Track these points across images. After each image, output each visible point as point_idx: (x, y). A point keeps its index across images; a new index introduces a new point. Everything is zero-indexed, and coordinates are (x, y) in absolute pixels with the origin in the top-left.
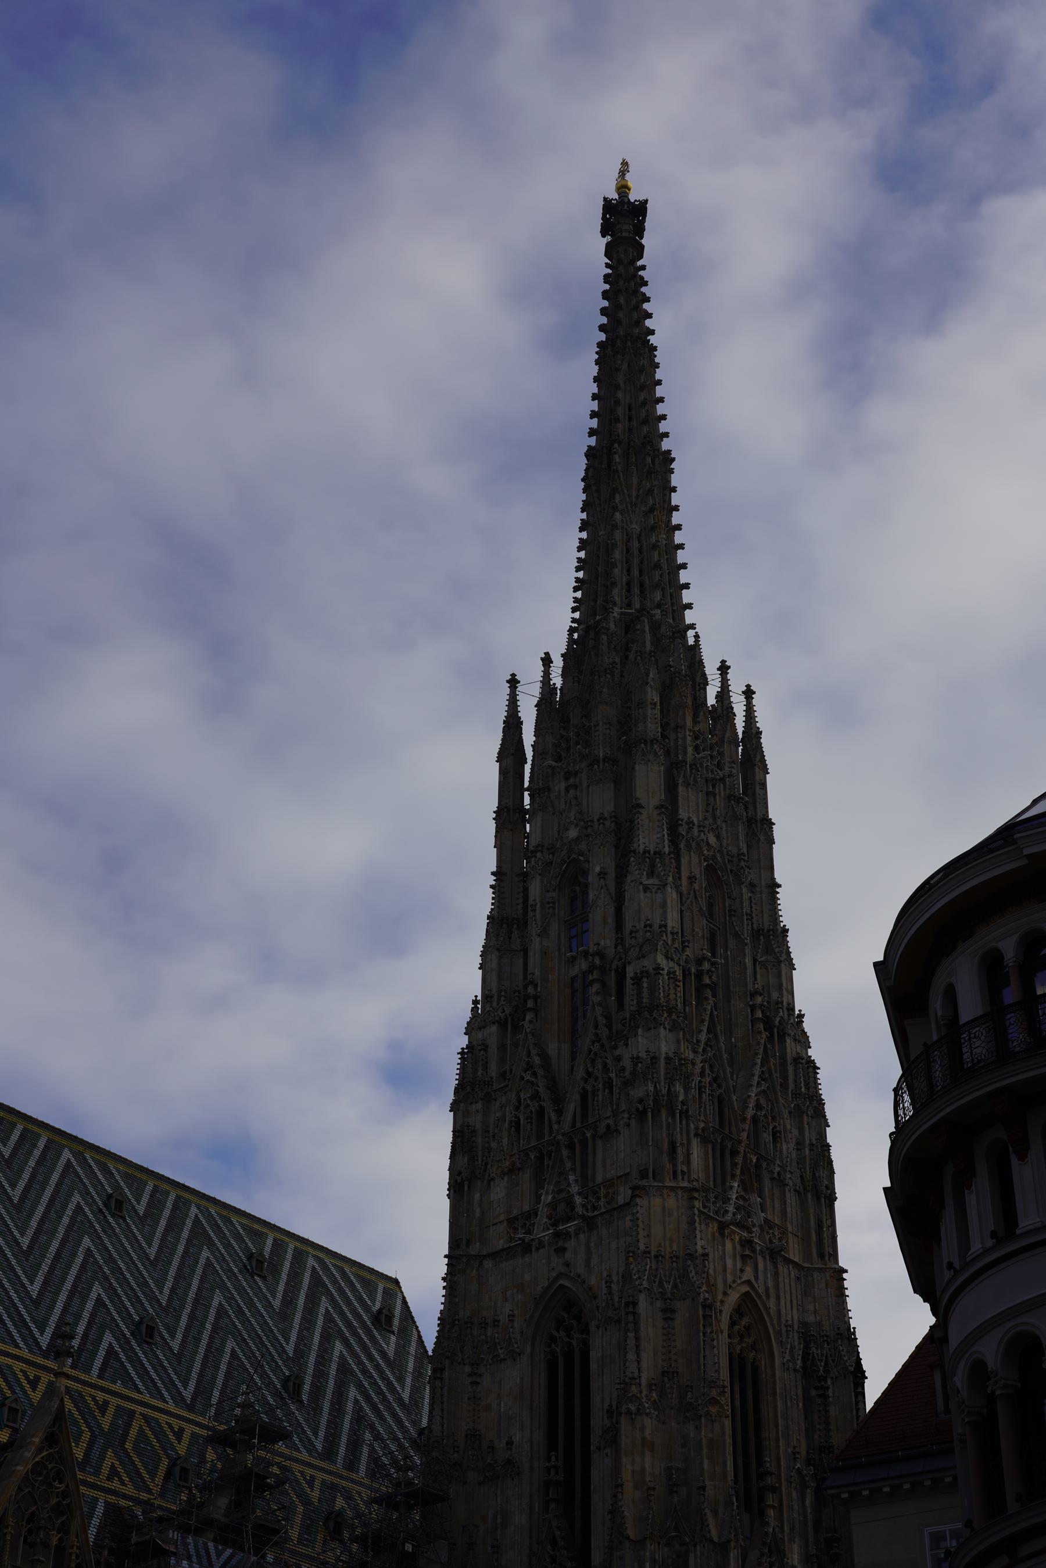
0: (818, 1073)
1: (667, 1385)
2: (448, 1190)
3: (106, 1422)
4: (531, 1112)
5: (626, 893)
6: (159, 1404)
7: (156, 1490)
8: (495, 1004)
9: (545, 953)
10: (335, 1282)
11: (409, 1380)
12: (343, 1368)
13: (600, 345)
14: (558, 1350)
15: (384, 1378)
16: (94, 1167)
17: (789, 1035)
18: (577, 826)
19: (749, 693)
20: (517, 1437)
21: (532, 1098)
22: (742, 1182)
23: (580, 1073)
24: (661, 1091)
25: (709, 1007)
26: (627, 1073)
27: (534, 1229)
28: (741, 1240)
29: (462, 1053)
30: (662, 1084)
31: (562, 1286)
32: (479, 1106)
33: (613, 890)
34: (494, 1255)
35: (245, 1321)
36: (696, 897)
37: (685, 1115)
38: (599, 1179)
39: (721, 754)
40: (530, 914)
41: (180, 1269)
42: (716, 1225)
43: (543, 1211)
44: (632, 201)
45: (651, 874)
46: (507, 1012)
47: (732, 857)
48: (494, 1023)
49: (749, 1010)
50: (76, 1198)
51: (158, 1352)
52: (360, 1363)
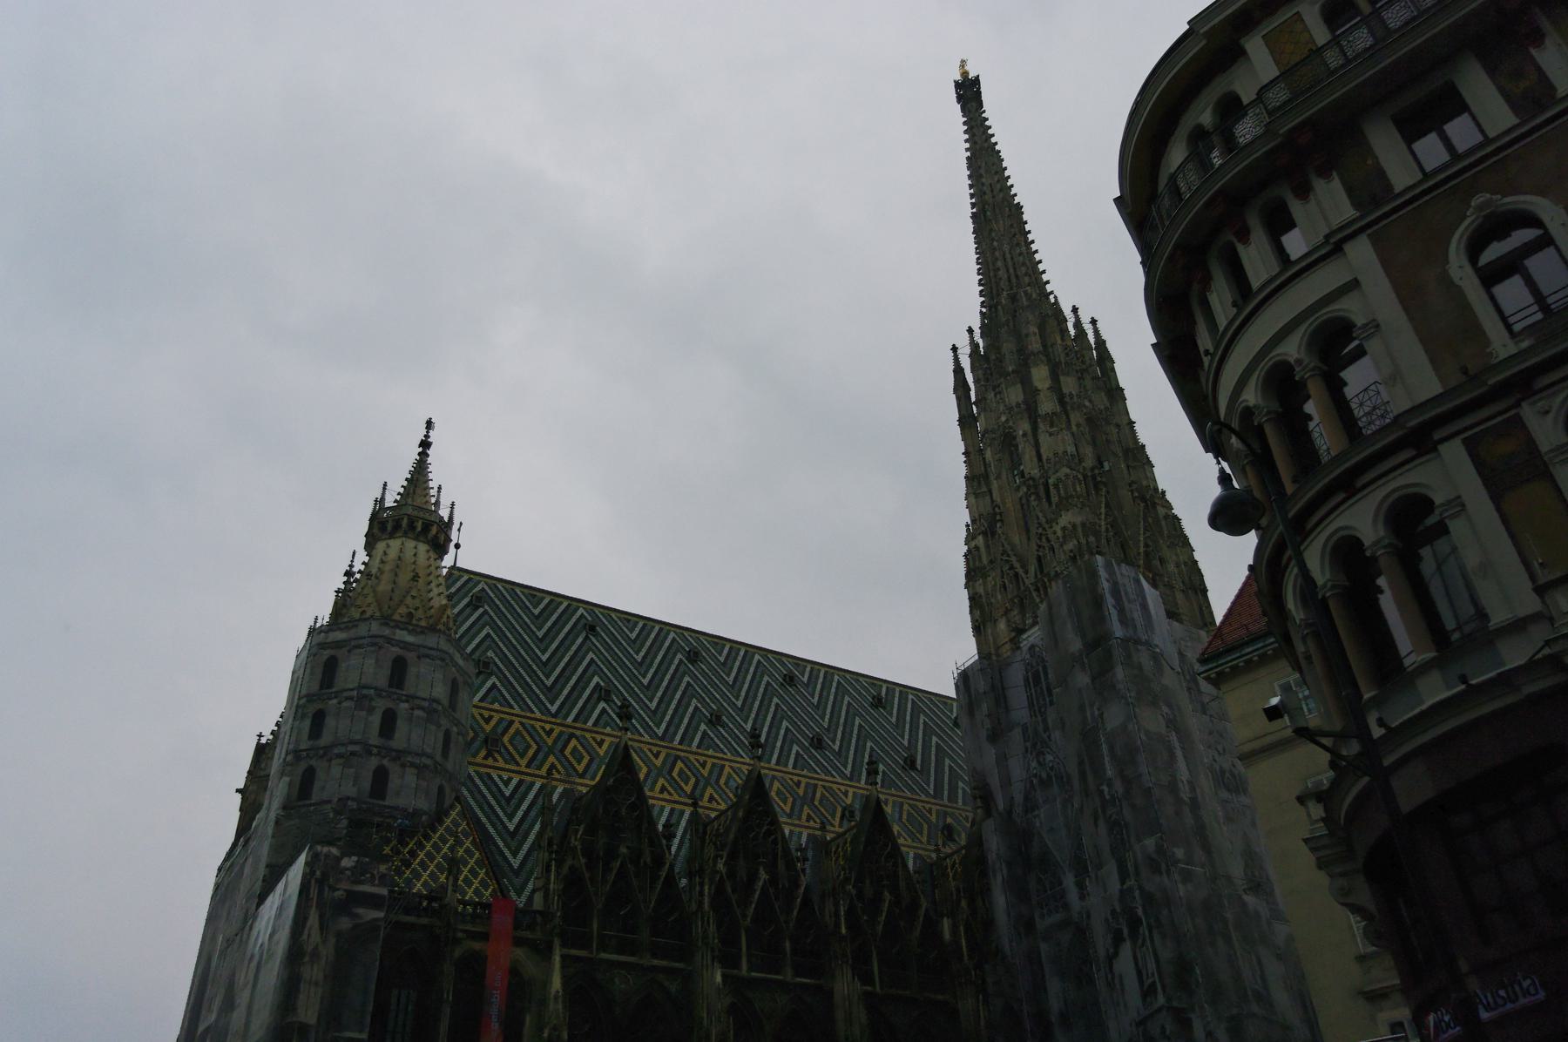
3: (801, 792)
6: (831, 779)
7: (837, 824)
13: (968, 158)
19: (1094, 322)
21: (1010, 569)
26: (1061, 540)
29: (965, 555)
32: (981, 581)
33: (1032, 442)
35: (876, 731)
39: (1083, 356)
40: (989, 469)
45: (1052, 425)
48: (979, 534)
50: (766, 678)
51: (827, 752)
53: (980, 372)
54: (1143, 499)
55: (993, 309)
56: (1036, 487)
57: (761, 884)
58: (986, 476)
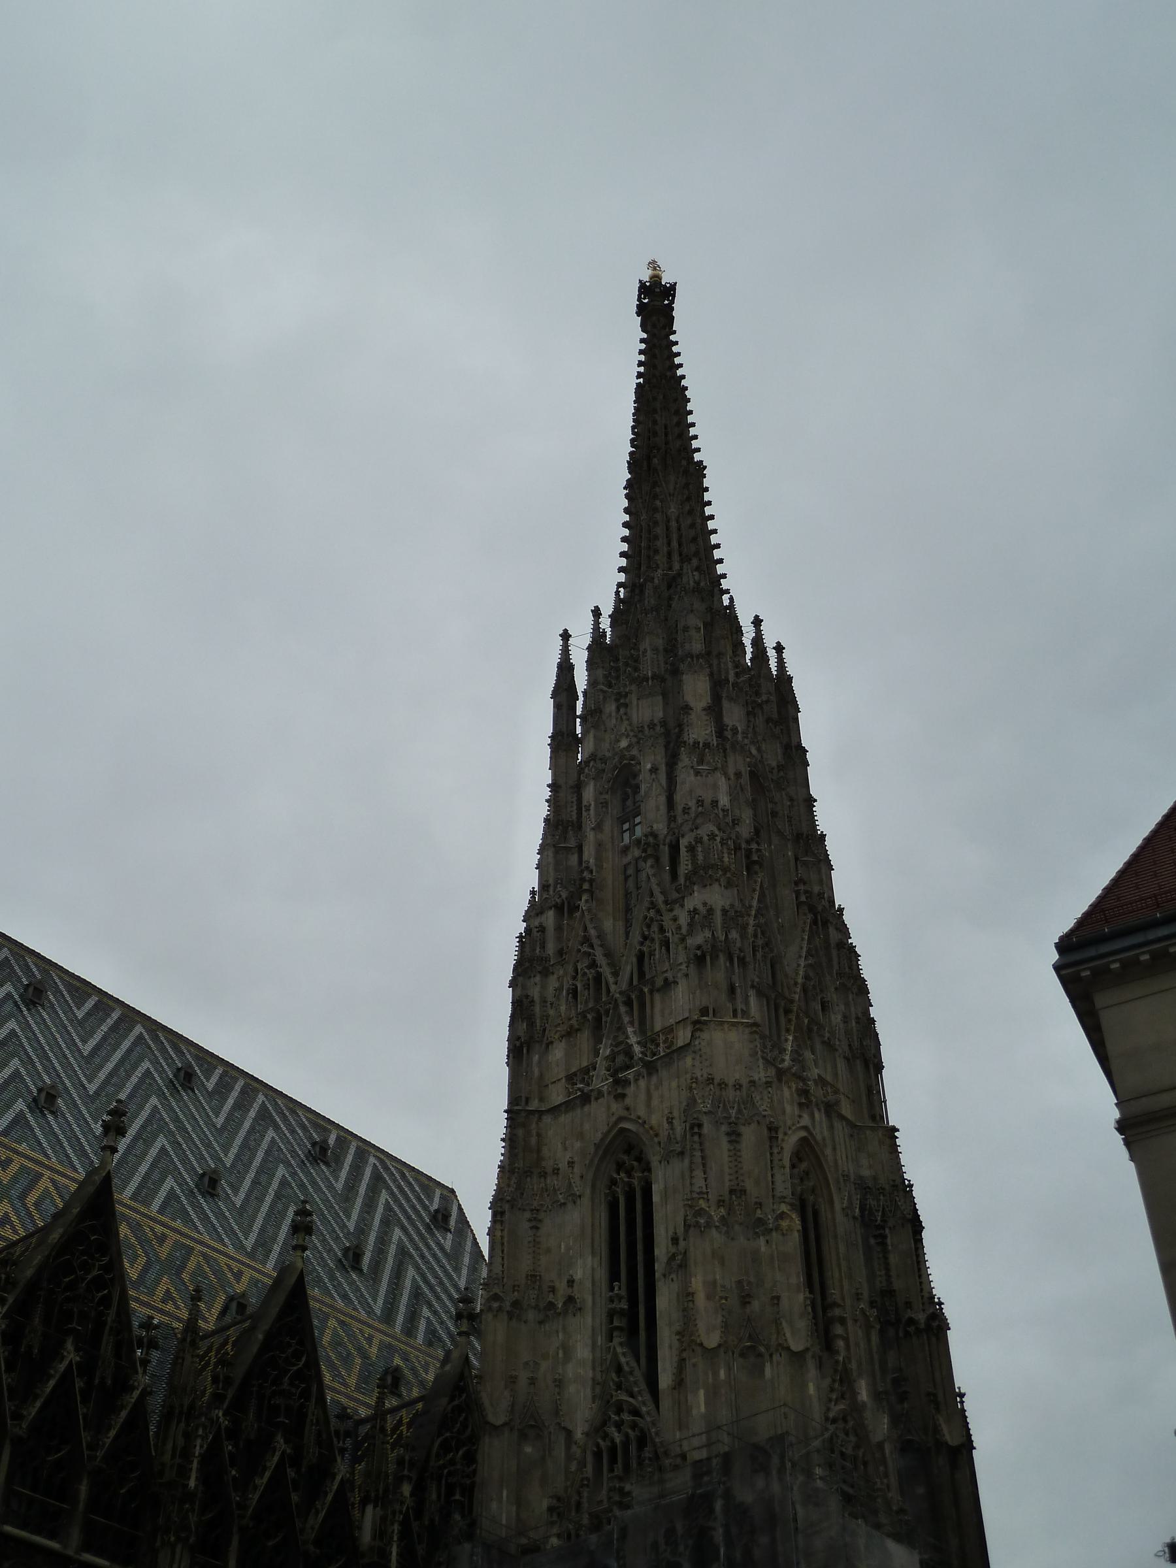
0: (859, 960)
1: (735, 1203)
2: (508, 1056)
3: (164, 1251)
4: (589, 979)
5: (677, 778)
8: (551, 892)
9: (600, 845)
10: (395, 1180)
11: (465, 1272)
12: (402, 1252)
14: (619, 1190)
15: (442, 1267)
16: (166, 1044)
17: (831, 923)
18: (627, 736)
19: (779, 648)
20: (578, 1274)
21: (589, 967)
22: (795, 1038)
23: (636, 937)
24: (718, 938)
25: (759, 880)
26: (684, 931)
27: (592, 1081)
28: (797, 1090)
29: (520, 937)
30: (720, 932)
31: (623, 1130)
32: (538, 979)
33: (664, 782)
34: (555, 1110)
36: (742, 790)
37: (743, 962)
38: (658, 1027)
40: (584, 814)
41: (246, 1139)
42: (772, 1072)
43: (601, 1063)
44: (663, 283)
46: (564, 895)
47: (773, 769)
48: (551, 908)
49: (794, 895)
52: (417, 1249)
53: (600, 673)
54: (812, 909)
55: (637, 591)
56: (656, 846)
57: (62, 1367)
58: (580, 827)
